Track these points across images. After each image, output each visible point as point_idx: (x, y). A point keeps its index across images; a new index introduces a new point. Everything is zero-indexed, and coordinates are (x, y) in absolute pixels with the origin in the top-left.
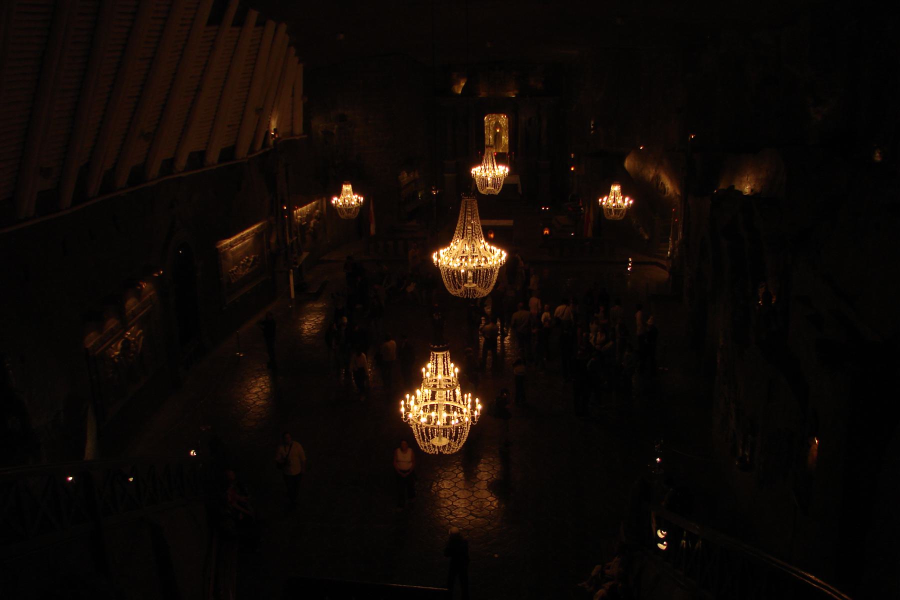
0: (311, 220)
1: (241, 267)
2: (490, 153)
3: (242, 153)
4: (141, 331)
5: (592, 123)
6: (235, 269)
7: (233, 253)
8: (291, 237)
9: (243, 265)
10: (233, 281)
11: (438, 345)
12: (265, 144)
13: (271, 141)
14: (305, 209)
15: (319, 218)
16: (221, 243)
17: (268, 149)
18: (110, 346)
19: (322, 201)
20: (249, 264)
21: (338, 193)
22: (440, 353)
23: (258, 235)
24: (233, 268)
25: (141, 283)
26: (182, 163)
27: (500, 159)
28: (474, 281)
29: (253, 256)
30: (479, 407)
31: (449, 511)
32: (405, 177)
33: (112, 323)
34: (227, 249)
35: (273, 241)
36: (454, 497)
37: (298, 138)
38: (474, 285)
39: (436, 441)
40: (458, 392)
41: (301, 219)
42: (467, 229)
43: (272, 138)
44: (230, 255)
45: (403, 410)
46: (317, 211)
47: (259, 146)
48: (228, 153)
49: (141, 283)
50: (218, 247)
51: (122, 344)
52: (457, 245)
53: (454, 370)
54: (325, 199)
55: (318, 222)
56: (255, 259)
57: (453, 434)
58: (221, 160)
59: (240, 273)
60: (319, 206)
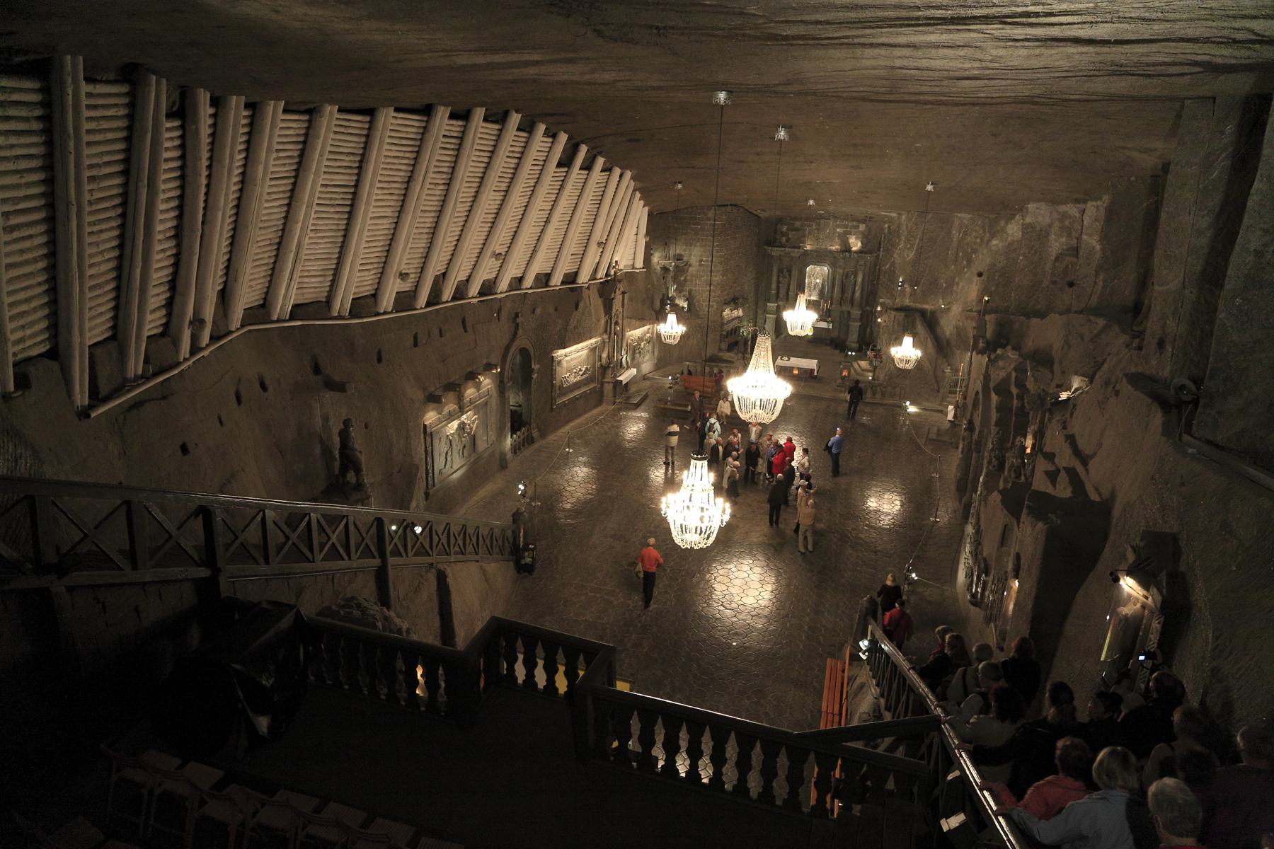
2: (802, 301)
3: (583, 278)
5: (901, 280)
7: (567, 361)
13: (612, 273)
18: (446, 425)
20: (581, 373)
21: (664, 319)
22: (699, 463)
26: (529, 281)
27: (810, 304)
30: (728, 511)
33: (452, 407)
35: (604, 355)
37: (638, 271)
44: (564, 364)
45: (663, 506)
47: (601, 274)
48: (571, 278)
51: (459, 425)
53: (711, 477)
56: (587, 368)
58: (563, 283)
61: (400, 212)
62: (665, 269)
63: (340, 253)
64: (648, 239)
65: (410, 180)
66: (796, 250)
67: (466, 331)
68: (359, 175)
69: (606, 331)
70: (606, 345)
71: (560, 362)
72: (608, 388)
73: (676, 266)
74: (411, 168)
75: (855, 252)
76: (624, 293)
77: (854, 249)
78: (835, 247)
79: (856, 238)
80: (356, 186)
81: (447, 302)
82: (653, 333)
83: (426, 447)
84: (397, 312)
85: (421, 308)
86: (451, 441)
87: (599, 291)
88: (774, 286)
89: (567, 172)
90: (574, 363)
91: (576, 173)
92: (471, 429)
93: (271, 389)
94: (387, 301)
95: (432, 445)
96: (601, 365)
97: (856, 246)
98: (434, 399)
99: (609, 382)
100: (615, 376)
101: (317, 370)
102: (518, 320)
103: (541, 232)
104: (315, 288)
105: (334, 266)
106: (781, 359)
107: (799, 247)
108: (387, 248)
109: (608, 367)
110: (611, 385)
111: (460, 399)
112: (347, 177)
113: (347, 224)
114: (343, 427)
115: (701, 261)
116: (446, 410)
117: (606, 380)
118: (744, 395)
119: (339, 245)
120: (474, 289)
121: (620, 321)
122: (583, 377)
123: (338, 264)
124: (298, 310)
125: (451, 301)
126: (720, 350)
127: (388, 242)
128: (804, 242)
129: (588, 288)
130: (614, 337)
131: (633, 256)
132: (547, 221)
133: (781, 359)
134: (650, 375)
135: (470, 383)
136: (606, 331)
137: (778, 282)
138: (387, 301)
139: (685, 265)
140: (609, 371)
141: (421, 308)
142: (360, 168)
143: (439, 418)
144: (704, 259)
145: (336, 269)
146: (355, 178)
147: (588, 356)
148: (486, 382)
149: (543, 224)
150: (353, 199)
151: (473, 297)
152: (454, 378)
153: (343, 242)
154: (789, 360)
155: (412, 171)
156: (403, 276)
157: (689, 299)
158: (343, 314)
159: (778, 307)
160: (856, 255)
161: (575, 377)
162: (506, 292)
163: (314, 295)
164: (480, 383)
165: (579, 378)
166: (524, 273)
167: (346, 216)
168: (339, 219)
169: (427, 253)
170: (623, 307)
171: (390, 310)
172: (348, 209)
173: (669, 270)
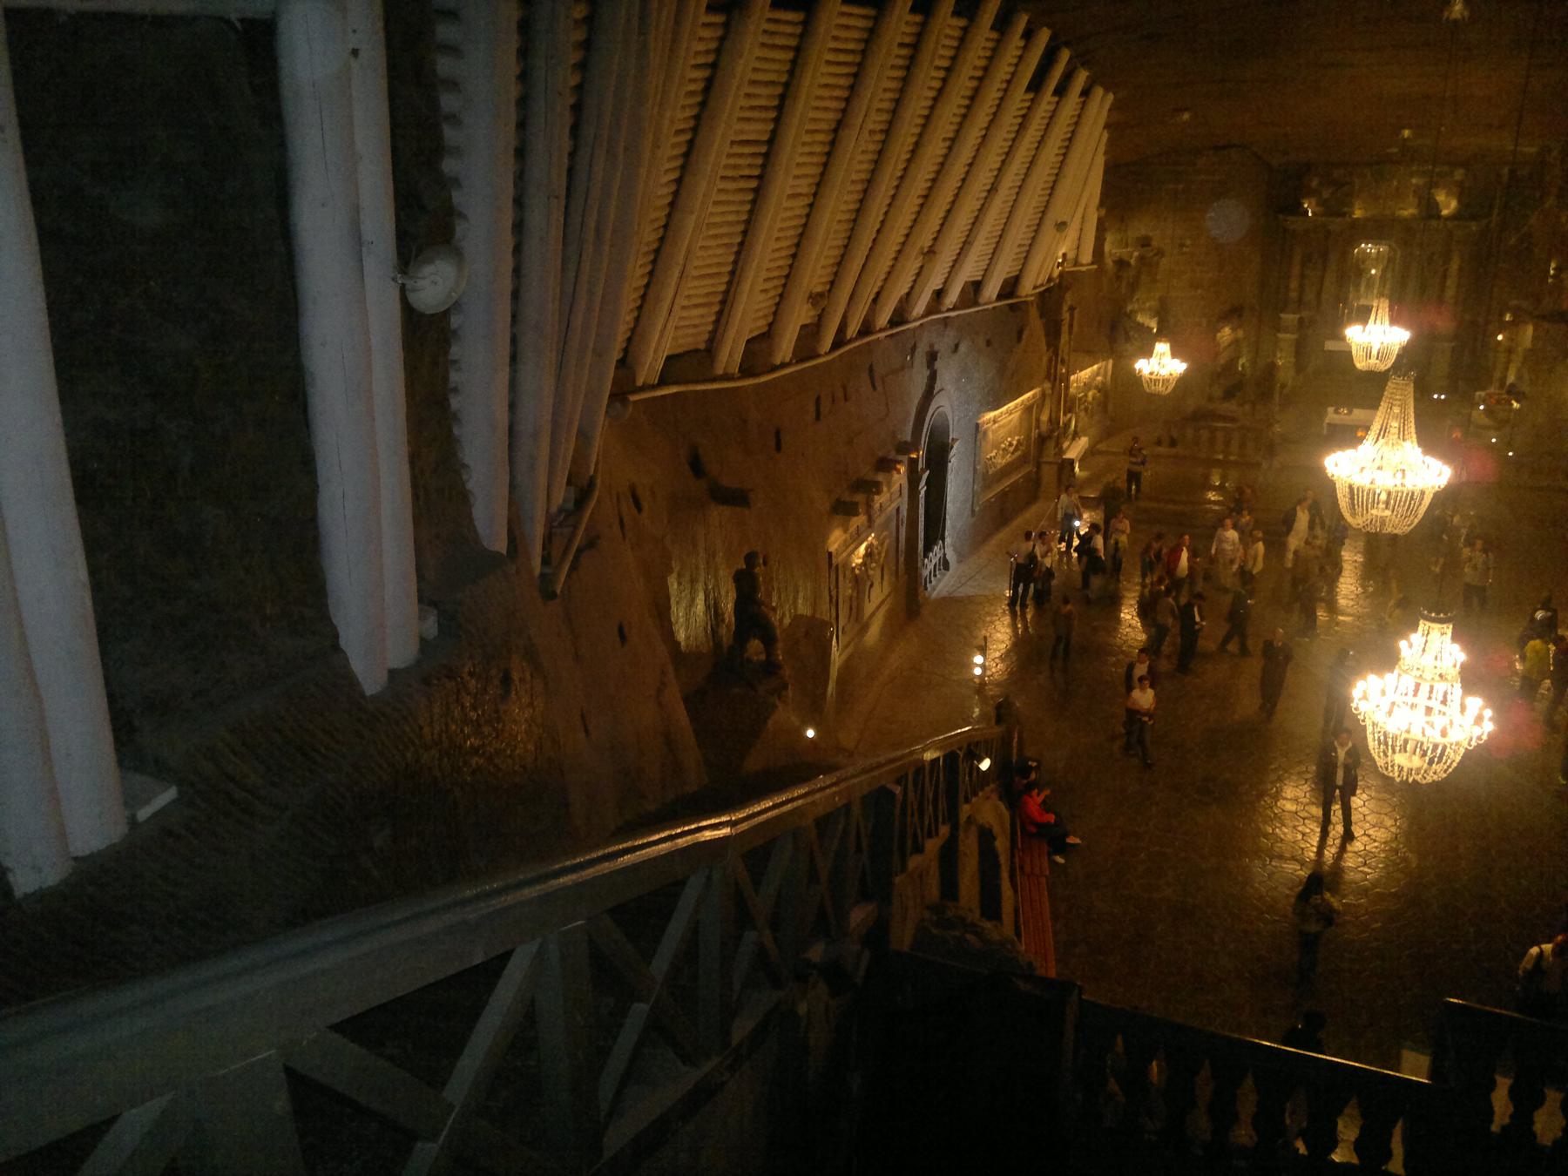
0: (1090, 390)
1: (1001, 452)
3: (1027, 289)
4: (885, 533)
6: (993, 454)
7: (995, 432)
8: (1065, 414)
9: (1004, 449)
10: (990, 473)
11: (1438, 613)
12: (1050, 279)
13: (1056, 273)
14: (1085, 374)
15: (1102, 389)
16: (983, 416)
17: (1052, 284)
18: (853, 552)
19: (1107, 364)
20: (1011, 449)
21: (1148, 352)
22: (1436, 626)
23: (1028, 409)
24: (992, 452)
25: (898, 466)
26: (952, 297)
28: (1387, 503)
29: (1016, 438)
31: (1360, 860)
32: (1226, 334)
33: (859, 520)
34: (989, 425)
35: (1044, 418)
36: (1366, 838)
37: (1084, 269)
38: (1388, 513)
39: (1400, 759)
40: (1457, 690)
41: (1077, 388)
42: (1391, 426)
43: (1058, 267)
44: (990, 435)
46: (1099, 378)
48: (1010, 287)
49: (898, 466)
50: (979, 422)
51: (866, 549)
52: (1368, 450)
54: (1111, 361)
55: (1098, 394)
56: (1019, 441)
57: (1436, 755)
58: (1000, 297)
59: (999, 461)
60: (1102, 371)
61: (818, 185)
62: (1121, 263)
63: (735, 263)
64: (1103, 212)
65: (839, 126)
66: (1339, 220)
67: (874, 387)
68: (777, 120)
69: (1048, 377)
70: (1048, 401)
71: (985, 433)
72: (1048, 474)
73: (1141, 258)
74: (843, 105)
75: (1447, 218)
76: (1072, 309)
77: (1445, 212)
78: (1408, 211)
79: (1448, 194)
80: (771, 142)
81: (851, 341)
82: (1106, 372)
83: (830, 592)
84: (797, 362)
85: (826, 354)
86: (856, 576)
87: (1037, 306)
88: (1294, 284)
89: (1032, 100)
90: (1002, 432)
91: (1047, 99)
92: (879, 553)
93: (645, 505)
94: (785, 347)
95: (837, 587)
96: (1040, 435)
97: (1447, 207)
98: (844, 509)
99: (1050, 463)
100: (1061, 452)
101: (696, 466)
102: (938, 365)
103: (980, 210)
104: (695, 326)
105: (723, 288)
106: (1336, 412)
107: (1344, 215)
108: (793, 251)
109: (1050, 437)
110: (1056, 467)
111: (869, 506)
112: (760, 126)
113: (751, 212)
114: (744, 567)
115: (1182, 245)
116: (852, 529)
117: (1045, 460)
118: (1361, 481)
119: (735, 249)
120: (883, 319)
121: (1066, 357)
122: (1014, 457)
123: (730, 283)
124: (674, 368)
125: (856, 339)
126: (1210, 399)
127: (796, 241)
128: (1351, 205)
129: (1032, 302)
130: (1056, 380)
131: (1076, 243)
132: (992, 190)
133: (1336, 412)
134: (1102, 447)
135: (880, 477)
136: (1048, 377)
137: (1302, 276)
138: (785, 347)
139: (1156, 255)
140: (1051, 445)
141: (826, 354)
142: (780, 108)
143: (845, 541)
144: (1188, 242)
145: (727, 292)
146: (771, 126)
147: (1021, 418)
148: (900, 476)
149: (984, 194)
150: (764, 166)
151: (881, 330)
152: (866, 472)
153: (742, 244)
154: (1350, 412)
155: (844, 111)
156: (815, 299)
157: (1162, 314)
158: (731, 371)
159: (1301, 321)
160: (1450, 224)
161: (1003, 457)
162: (923, 316)
163: (690, 339)
164: (892, 476)
165: (1008, 458)
166: (945, 282)
167: (750, 197)
168: (742, 203)
169: (843, 256)
170: (1070, 333)
171: (787, 360)
172: (753, 184)
173: (1129, 264)
